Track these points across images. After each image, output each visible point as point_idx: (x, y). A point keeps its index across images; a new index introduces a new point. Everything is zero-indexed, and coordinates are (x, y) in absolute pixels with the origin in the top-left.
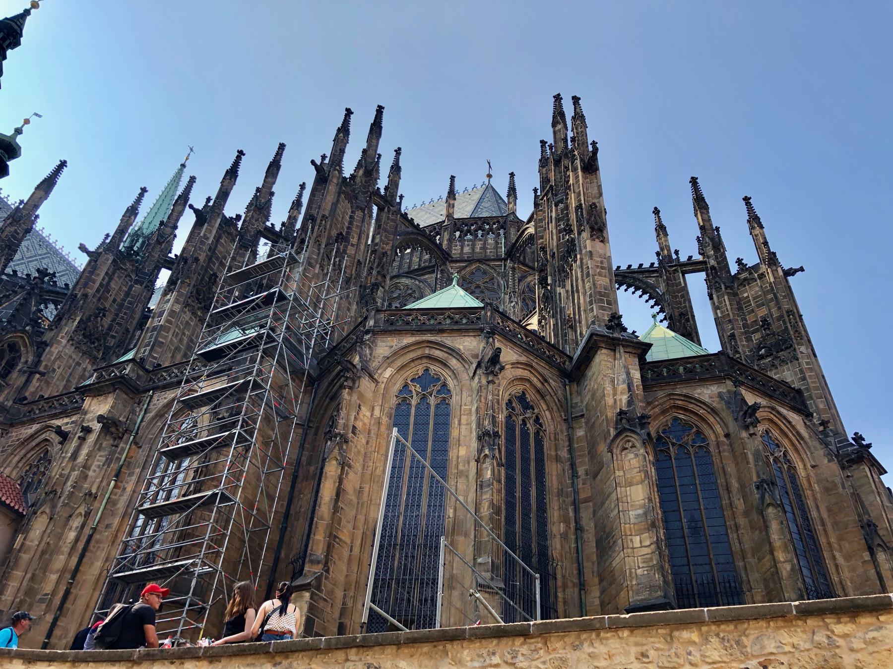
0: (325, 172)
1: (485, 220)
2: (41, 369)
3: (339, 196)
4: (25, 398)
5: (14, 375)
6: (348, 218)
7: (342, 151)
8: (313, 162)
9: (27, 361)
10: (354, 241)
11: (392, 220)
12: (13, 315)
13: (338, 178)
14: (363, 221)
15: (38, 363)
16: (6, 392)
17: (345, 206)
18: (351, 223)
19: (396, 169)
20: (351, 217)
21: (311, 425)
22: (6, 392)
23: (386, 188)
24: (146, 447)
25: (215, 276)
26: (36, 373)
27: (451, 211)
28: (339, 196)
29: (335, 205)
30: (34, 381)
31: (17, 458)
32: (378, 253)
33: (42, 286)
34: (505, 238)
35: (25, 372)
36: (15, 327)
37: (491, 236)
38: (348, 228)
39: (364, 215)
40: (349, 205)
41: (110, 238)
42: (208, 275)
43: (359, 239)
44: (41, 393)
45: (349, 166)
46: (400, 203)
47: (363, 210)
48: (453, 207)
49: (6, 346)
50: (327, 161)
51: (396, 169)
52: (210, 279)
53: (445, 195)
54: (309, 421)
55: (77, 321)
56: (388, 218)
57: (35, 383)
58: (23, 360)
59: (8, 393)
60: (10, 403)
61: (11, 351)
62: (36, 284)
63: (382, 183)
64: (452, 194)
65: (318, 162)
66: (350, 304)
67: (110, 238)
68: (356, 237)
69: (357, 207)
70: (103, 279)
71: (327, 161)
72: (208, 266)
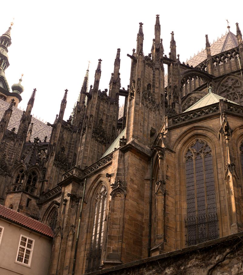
0: (136, 58)
1: (227, 52)
2: (47, 179)
3: (145, 66)
4: (44, 192)
5: (37, 184)
6: (152, 75)
7: (142, 45)
8: (128, 55)
9: (40, 177)
10: (157, 85)
11: (176, 69)
12: (30, 160)
13: (142, 58)
14: (160, 75)
15: (44, 177)
16: (36, 191)
17: (149, 70)
18: (154, 77)
19: (173, 43)
20: (154, 74)
21: (153, 178)
22: (36, 191)
23: (170, 54)
24: (89, 203)
25: (102, 120)
26: (44, 181)
27: (209, 53)
28: (145, 66)
29: (143, 72)
30: (46, 184)
31: (47, 216)
32: (172, 87)
33: (38, 146)
34: (240, 58)
35: (40, 182)
36: (32, 165)
37: (232, 59)
38: (153, 80)
39: (160, 72)
40: (151, 69)
41: (58, 116)
42: (99, 121)
43: (159, 84)
44: (49, 189)
45: (147, 50)
46: (178, 59)
47: (158, 69)
48: (210, 50)
49: (31, 173)
50: (136, 52)
51: (173, 43)
52: (100, 122)
53: (204, 47)
54: (152, 177)
55: (54, 156)
56: (174, 68)
57: (46, 185)
58: (39, 177)
59: (37, 192)
60: (38, 196)
61: (33, 175)
62: (35, 145)
63: (167, 52)
64: (208, 45)
65: (131, 54)
66: (162, 116)
67: (58, 116)
68: (158, 83)
69: (156, 68)
70: (60, 135)
71: (136, 52)
72: (98, 117)
